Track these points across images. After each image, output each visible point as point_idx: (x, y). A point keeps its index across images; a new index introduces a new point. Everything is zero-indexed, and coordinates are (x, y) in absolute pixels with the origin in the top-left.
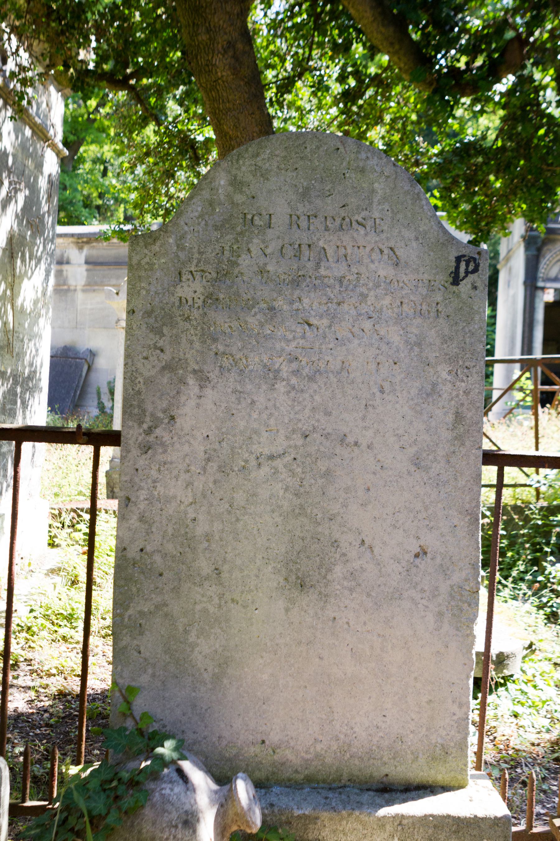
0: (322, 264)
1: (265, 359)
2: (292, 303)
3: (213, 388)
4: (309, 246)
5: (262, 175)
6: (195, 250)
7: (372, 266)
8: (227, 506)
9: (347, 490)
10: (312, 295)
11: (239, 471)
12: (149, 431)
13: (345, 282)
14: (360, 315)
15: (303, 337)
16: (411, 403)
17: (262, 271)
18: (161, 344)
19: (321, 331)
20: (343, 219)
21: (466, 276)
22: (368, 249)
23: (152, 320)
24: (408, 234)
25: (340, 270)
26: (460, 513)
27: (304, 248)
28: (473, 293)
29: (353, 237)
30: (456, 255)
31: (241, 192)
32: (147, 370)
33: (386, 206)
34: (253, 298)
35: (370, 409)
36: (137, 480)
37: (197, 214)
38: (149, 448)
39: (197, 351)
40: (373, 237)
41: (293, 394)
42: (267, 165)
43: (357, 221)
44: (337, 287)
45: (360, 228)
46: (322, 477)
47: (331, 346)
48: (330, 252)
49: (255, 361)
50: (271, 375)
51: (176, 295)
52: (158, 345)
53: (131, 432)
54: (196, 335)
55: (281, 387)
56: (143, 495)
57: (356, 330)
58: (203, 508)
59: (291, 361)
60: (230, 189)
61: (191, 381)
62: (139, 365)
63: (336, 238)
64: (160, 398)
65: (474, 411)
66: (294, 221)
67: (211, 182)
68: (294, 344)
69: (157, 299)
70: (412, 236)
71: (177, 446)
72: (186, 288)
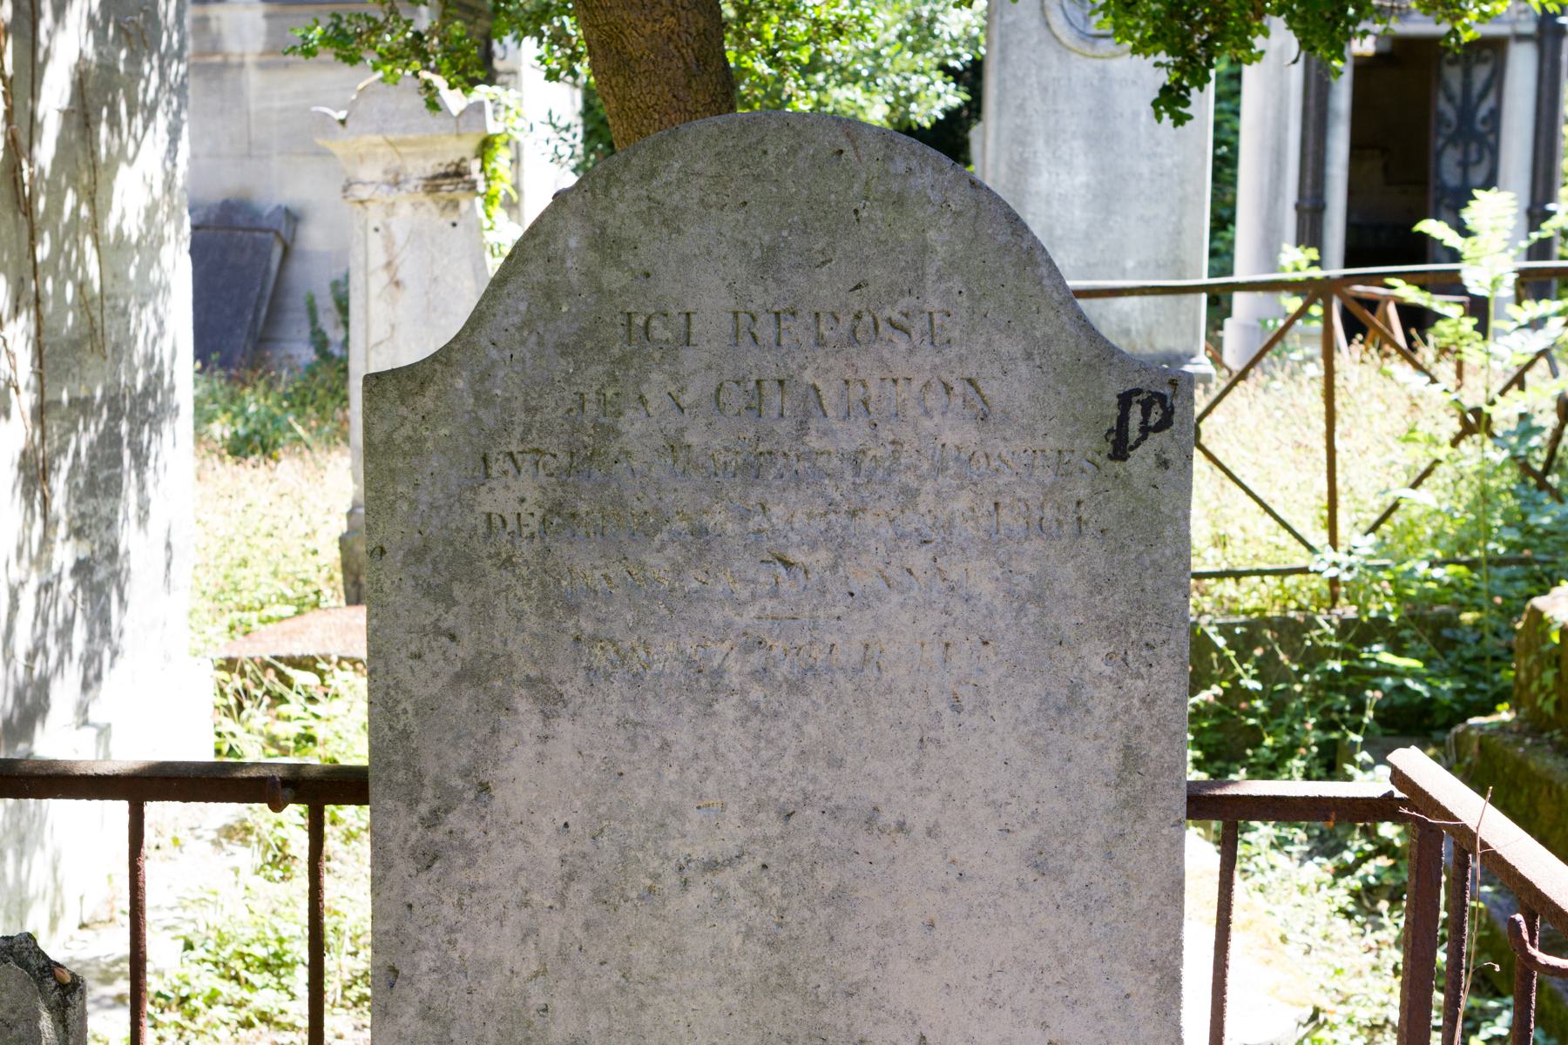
0: (813, 424)
1: (689, 645)
2: (745, 516)
3: (574, 716)
4: (781, 383)
5: (665, 223)
6: (517, 404)
7: (927, 424)
8: (617, 976)
9: (885, 929)
10: (791, 496)
11: (641, 898)
12: (433, 820)
13: (866, 464)
14: (902, 537)
15: (775, 594)
16: (1023, 729)
17: (674, 446)
18: (449, 622)
19: (814, 577)
20: (858, 317)
21: (1144, 438)
22: (916, 385)
23: (425, 571)
24: (1009, 346)
25: (852, 435)
26: (1139, 967)
27: (769, 388)
28: (1159, 475)
29: (881, 360)
30: (1120, 389)
31: (619, 264)
32: (422, 683)
33: (957, 284)
34: (657, 510)
35: (931, 748)
36: (410, 928)
37: (517, 319)
38: (435, 858)
39: (534, 635)
40: (926, 357)
41: (755, 723)
42: (677, 197)
43: (890, 321)
44: (848, 475)
45: (898, 338)
46: (826, 904)
47: (837, 611)
48: (829, 395)
49: (665, 652)
50: (704, 683)
51: (478, 509)
52: (444, 625)
53: (392, 823)
54: (529, 599)
55: (727, 708)
56: (426, 960)
57: (893, 572)
58: (563, 984)
59: (747, 650)
60: (592, 256)
61: (523, 704)
62: (403, 673)
63: (842, 364)
64: (455, 745)
65: (1164, 741)
66: (743, 328)
67: (547, 243)
68: (752, 611)
69: (435, 521)
70: (1017, 351)
71: (498, 849)
72: (500, 493)
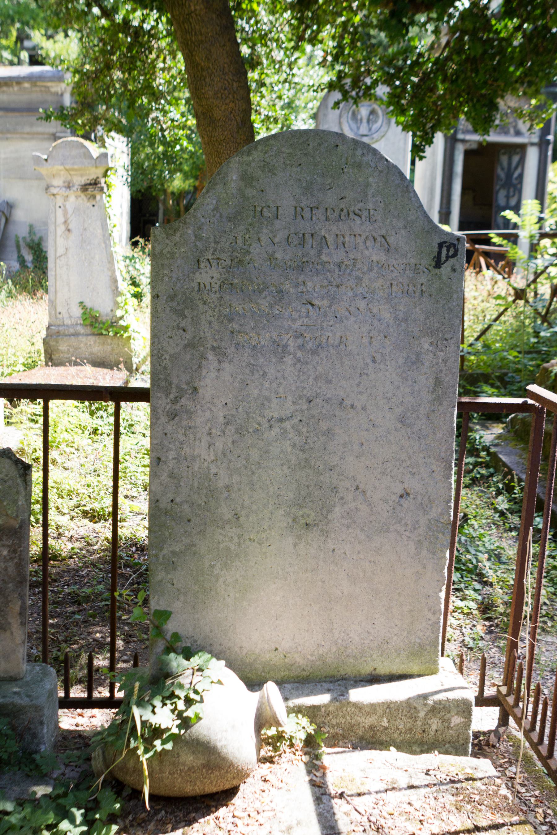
0: (324, 251)
2: (297, 287)
3: (230, 362)
5: (270, 171)
8: (244, 462)
9: (345, 445)
10: (315, 279)
11: (254, 432)
12: (175, 401)
13: (343, 267)
14: (356, 295)
15: (307, 316)
16: (399, 370)
17: (271, 258)
18: (183, 324)
19: (322, 310)
22: (364, 237)
25: (338, 256)
26: (438, 460)
27: (308, 237)
29: (350, 227)
30: (439, 241)
31: (252, 187)
32: (172, 348)
33: (379, 198)
34: (264, 283)
35: (364, 377)
36: (166, 443)
38: (176, 416)
39: (215, 330)
40: (368, 227)
41: (298, 366)
42: (275, 161)
44: (337, 271)
45: (356, 218)
46: (323, 435)
47: (330, 323)
48: (331, 240)
49: (265, 338)
50: (280, 350)
52: (181, 325)
53: (160, 402)
54: (214, 316)
55: (288, 359)
56: (172, 454)
57: (352, 309)
58: (224, 465)
59: (296, 338)
60: (242, 183)
61: (210, 356)
62: (165, 344)
63: (335, 228)
64: (184, 372)
65: (450, 376)
66: (298, 212)
67: (224, 177)
68: (299, 323)
69: (179, 285)
70: (401, 225)
71: (200, 412)
72: (204, 275)
